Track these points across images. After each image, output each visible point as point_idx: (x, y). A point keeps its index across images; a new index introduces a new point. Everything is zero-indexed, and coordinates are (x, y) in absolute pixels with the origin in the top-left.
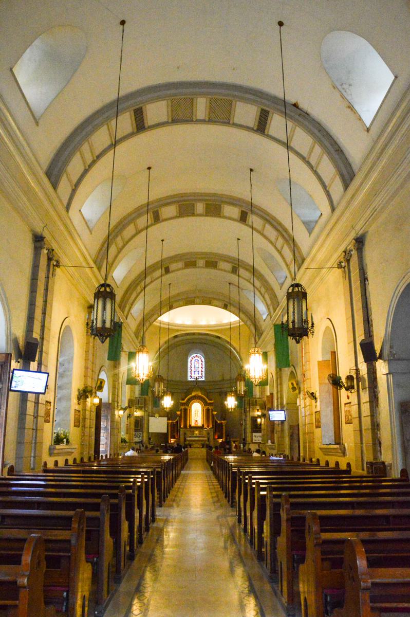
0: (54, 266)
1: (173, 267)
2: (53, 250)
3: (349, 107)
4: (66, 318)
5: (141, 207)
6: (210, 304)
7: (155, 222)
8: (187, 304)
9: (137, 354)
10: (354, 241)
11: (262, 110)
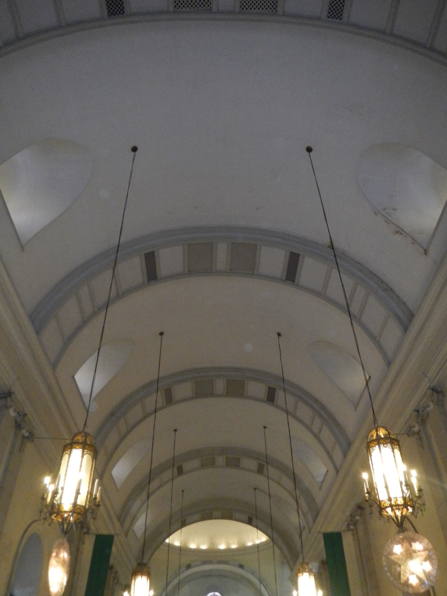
0: (24, 437)
1: (187, 466)
2: (25, 415)
3: (397, 232)
4: (35, 521)
5: (150, 384)
6: (230, 518)
7: (166, 404)
8: (203, 518)
9: (133, 581)
10: (429, 391)
11: (292, 253)
